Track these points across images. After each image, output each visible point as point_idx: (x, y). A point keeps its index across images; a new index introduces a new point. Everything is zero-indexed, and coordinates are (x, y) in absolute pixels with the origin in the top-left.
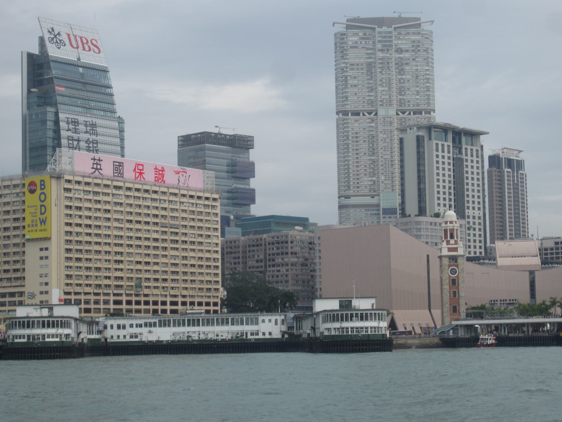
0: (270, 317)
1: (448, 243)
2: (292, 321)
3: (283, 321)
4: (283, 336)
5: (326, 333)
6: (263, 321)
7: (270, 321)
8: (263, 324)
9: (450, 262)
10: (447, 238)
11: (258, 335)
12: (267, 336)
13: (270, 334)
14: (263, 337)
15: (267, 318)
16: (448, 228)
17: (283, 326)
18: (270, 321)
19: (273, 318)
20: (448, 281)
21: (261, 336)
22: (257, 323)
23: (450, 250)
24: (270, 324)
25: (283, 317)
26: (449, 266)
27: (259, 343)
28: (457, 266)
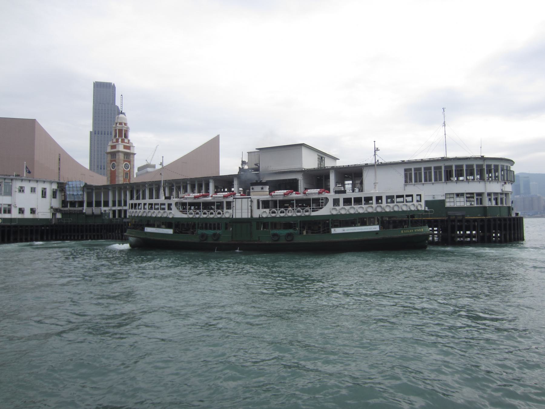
0: (33, 185)
1: (123, 141)
2: (81, 193)
3: (54, 195)
4: (54, 215)
5: (461, 203)
6: (22, 190)
7: (33, 190)
8: (21, 195)
9: (124, 158)
10: (122, 137)
11: (10, 212)
12: (28, 215)
13: (33, 211)
14: (20, 216)
15: (28, 186)
16: (124, 129)
17: (54, 200)
18: (33, 190)
19: (39, 187)
20: (122, 174)
21: (15, 214)
22: (9, 193)
23: (125, 147)
24: (33, 195)
25: (55, 186)
26: (124, 161)
27: (15, 226)
28: (130, 162)
